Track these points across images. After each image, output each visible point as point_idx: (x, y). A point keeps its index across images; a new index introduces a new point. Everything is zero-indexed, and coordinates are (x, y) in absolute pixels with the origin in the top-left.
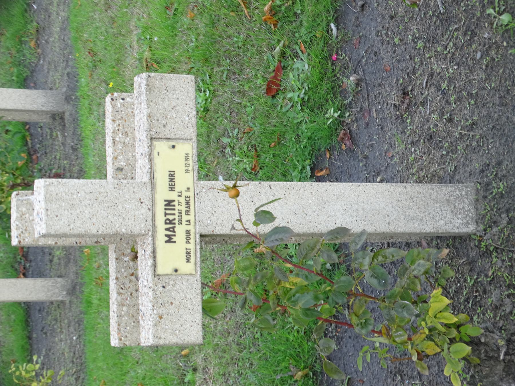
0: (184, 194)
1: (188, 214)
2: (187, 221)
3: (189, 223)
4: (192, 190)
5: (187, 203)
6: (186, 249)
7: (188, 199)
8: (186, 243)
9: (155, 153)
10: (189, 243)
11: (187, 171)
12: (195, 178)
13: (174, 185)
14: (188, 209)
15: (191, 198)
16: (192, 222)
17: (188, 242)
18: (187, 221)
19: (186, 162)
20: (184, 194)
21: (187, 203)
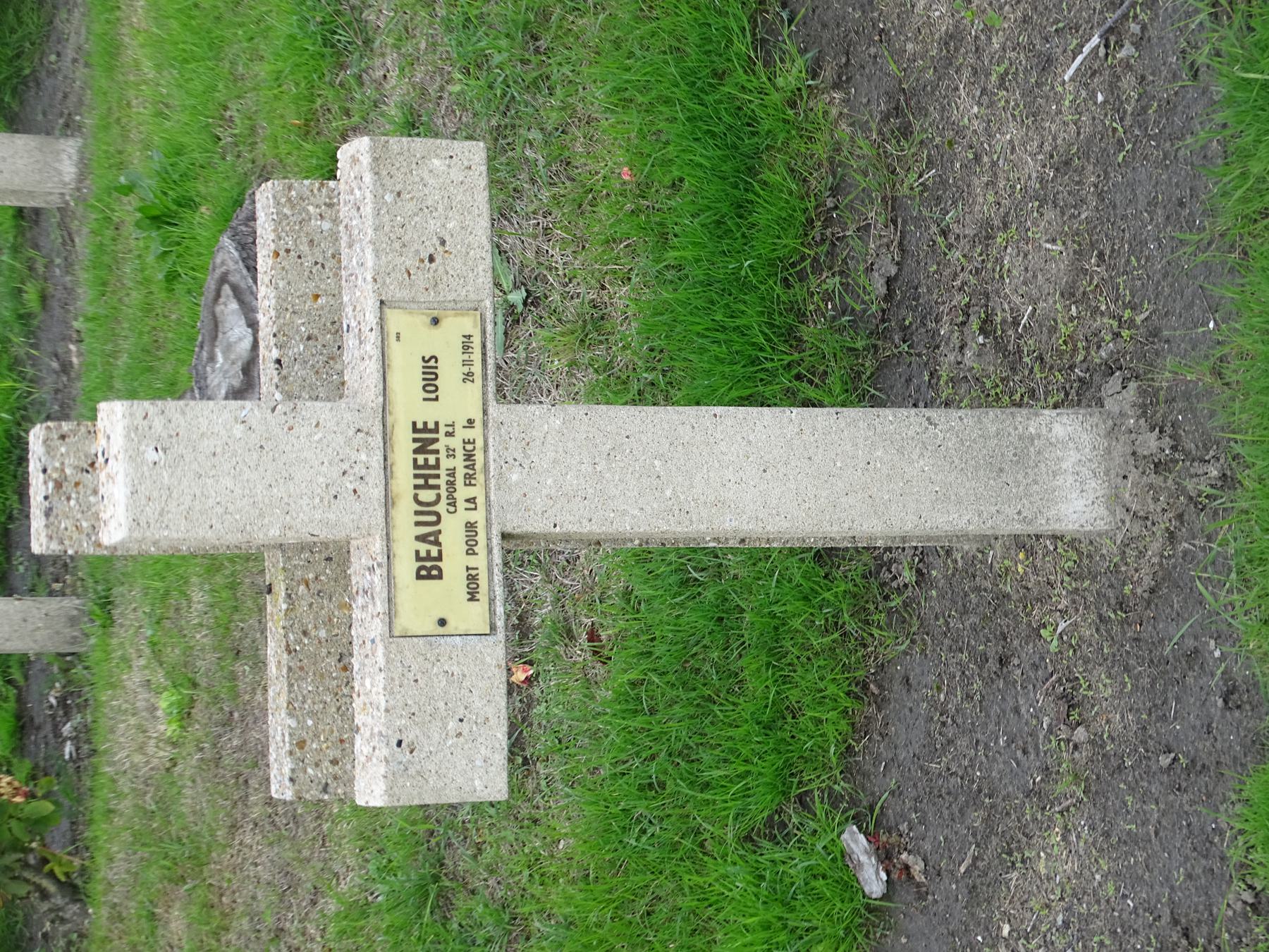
0: (462, 434)
1: (470, 484)
2: (468, 501)
3: (473, 506)
4: (478, 424)
5: (469, 456)
6: (468, 569)
7: (469, 447)
9: (393, 338)
11: (468, 377)
12: (491, 396)
14: (471, 472)
15: (480, 443)
16: (481, 501)
17: (471, 552)
18: (468, 501)
19: (466, 357)
20: (462, 434)
21: (469, 456)
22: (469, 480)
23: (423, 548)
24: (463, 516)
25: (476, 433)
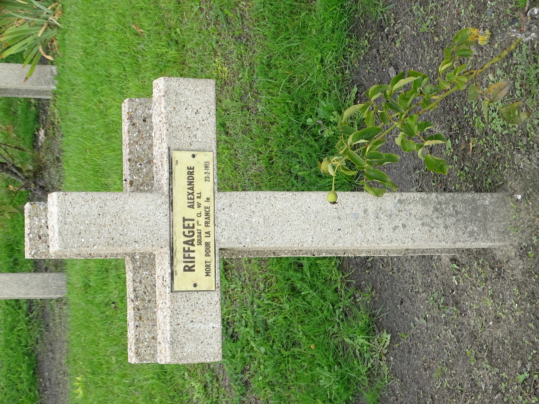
0: (204, 204)
2: (206, 233)
3: (208, 235)
4: (212, 200)
5: (207, 214)
7: (207, 210)
8: (206, 256)
9: (174, 163)
10: (209, 256)
11: (207, 179)
12: (216, 188)
13: (193, 199)
14: (208, 221)
17: (207, 255)
18: (206, 233)
19: (206, 171)
21: (207, 214)
22: (207, 224)
23: (187, 247)
24: (204, 240)
25: (211, 204)
